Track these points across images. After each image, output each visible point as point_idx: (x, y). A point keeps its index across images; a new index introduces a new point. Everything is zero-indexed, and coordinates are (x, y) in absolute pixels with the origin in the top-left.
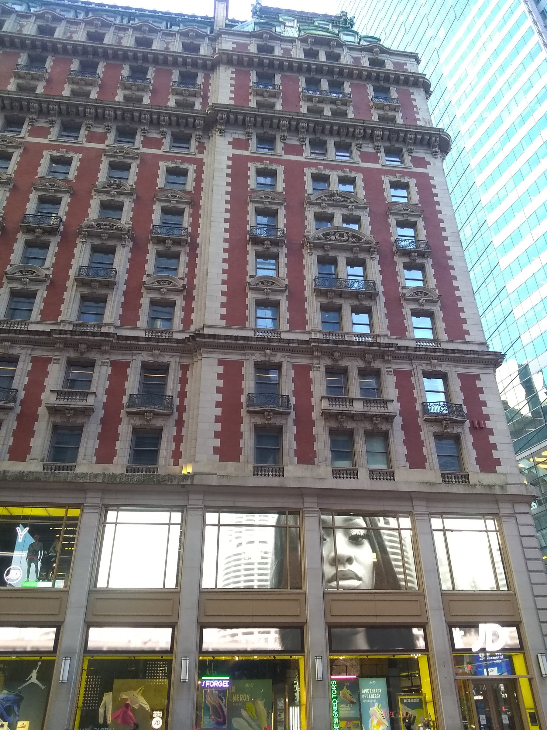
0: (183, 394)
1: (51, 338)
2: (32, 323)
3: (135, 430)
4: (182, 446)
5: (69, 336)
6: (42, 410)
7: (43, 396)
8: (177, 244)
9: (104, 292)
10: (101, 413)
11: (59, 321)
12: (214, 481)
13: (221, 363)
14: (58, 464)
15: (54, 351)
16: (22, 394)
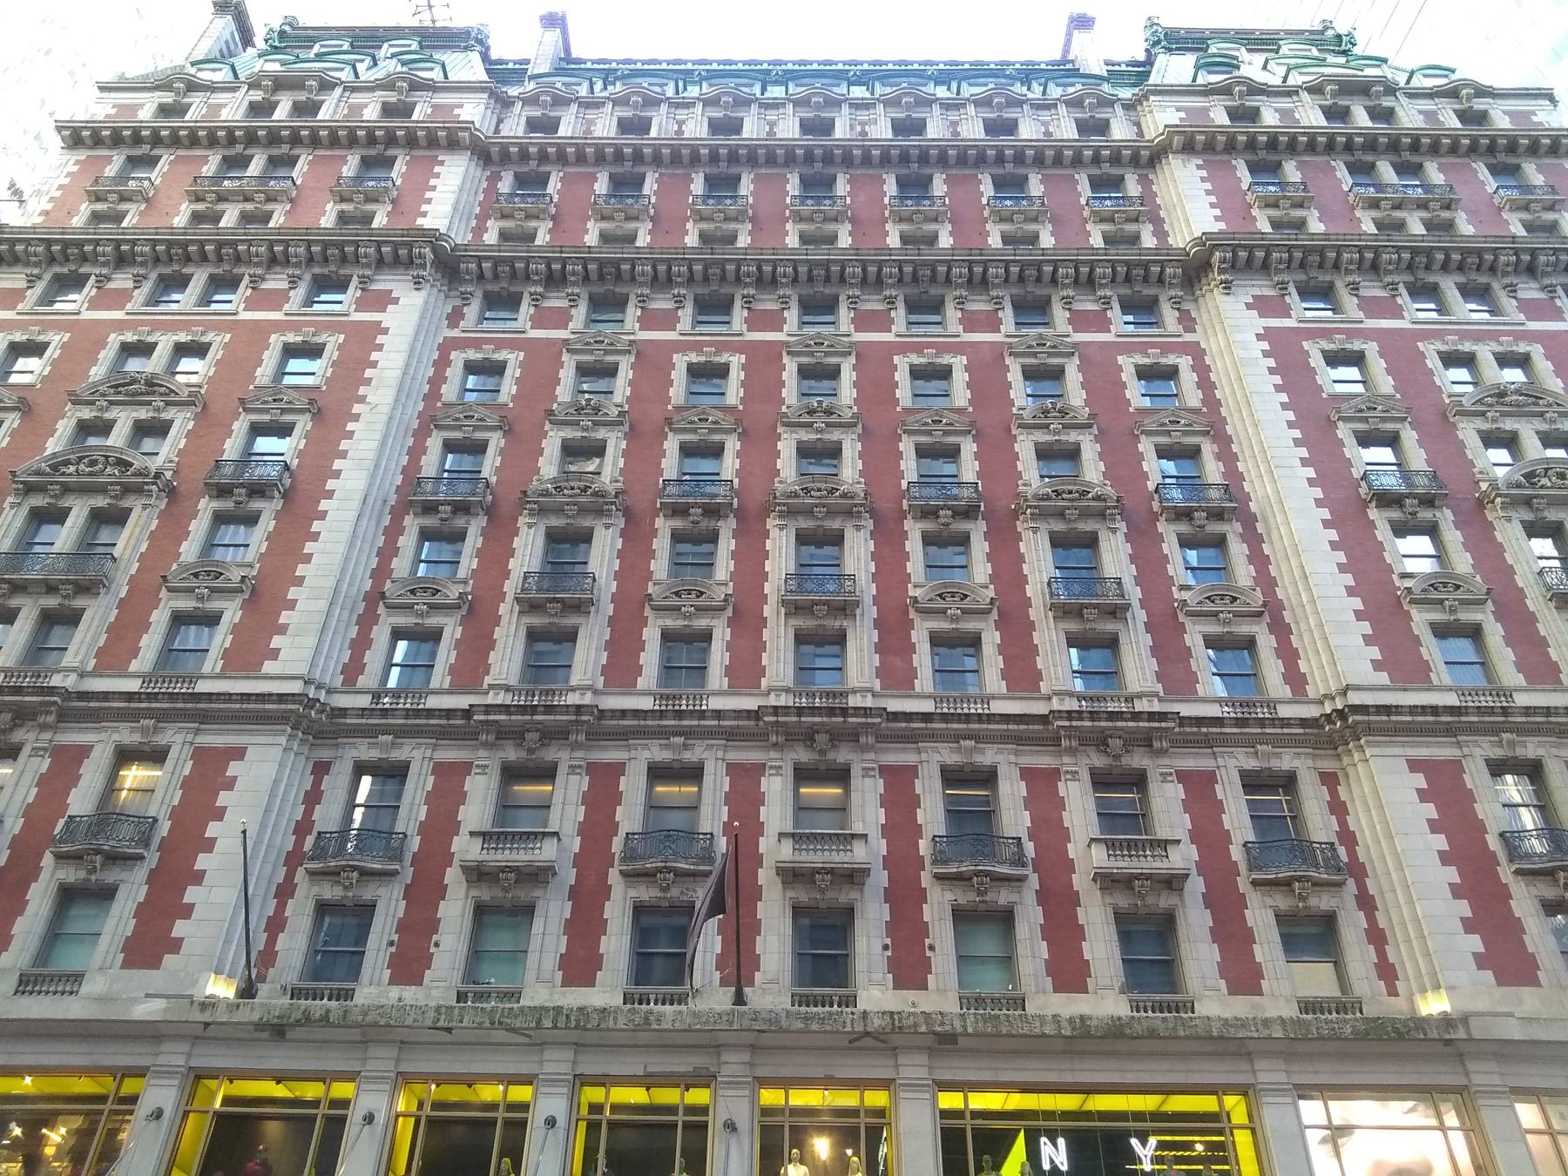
0: (1348, 838)
3: (1281, 918)
5: (1089, 724)
6: (1080, 881)
8: (1215, 519)
9: (1109, 626)
10: (1196, 886)
12: (1514, 1032)
13: (1415, 765)
14: (1158, 997)
15: (1059, 754)
16: (1029, 848)
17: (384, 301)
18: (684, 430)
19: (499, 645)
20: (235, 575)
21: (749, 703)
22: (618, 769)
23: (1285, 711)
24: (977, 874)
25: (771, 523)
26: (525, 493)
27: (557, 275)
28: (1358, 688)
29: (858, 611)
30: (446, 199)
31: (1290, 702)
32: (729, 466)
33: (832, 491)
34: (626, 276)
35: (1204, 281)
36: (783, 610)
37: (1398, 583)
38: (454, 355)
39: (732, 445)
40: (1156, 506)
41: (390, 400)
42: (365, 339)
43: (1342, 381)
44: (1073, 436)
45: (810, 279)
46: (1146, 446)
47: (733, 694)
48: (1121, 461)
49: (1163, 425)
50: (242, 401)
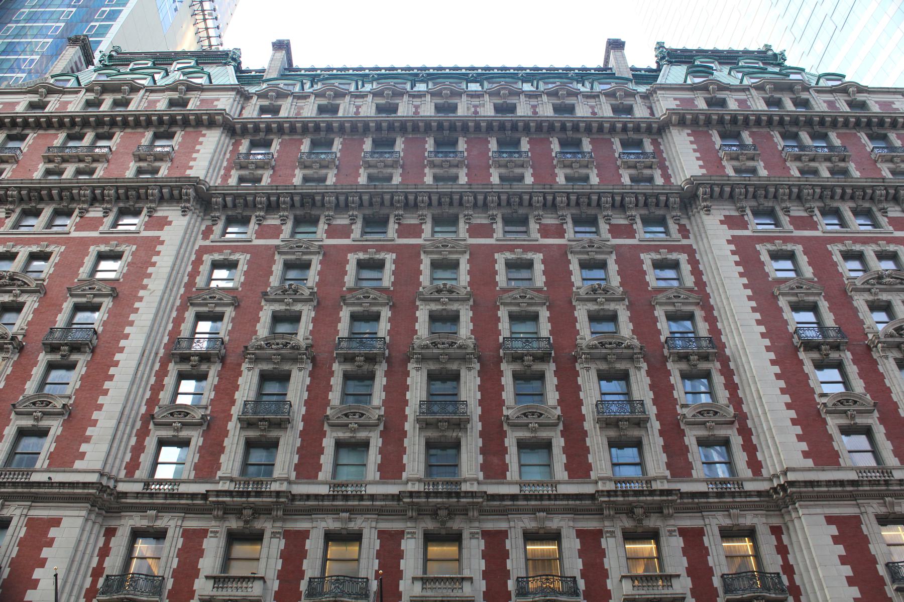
0: (788, 569)
9: (635, 433)
13: (830, 520)
15: (602, 520)
16: (581, 584)
17: (163, 223)
18: (353, 304)
19: (227, 450)
20: (59, 404)
21: (393, 489)
22: (305, 534)
23: (749, 486)
25: (410, 366)
26: (246, 348)
27: (274, 204)
29: (469, 426)
30: (205, 158)
32: (383, 328)
33: (452, 344)
34: (319, 204)
35: (694, 206)
36: (418, 426)
37: (818, 400)
38: (205, 257)
39: (386, 313)
40: (666, 352)
41: (162, 287)
42: (148, 248)
43: (779, 270)
44: (612, 306)
45: (440, 204)
46: (659, 312)
47: (383, 483)
48: (644, 322)
49: (670, 298)
50: (69, 289)
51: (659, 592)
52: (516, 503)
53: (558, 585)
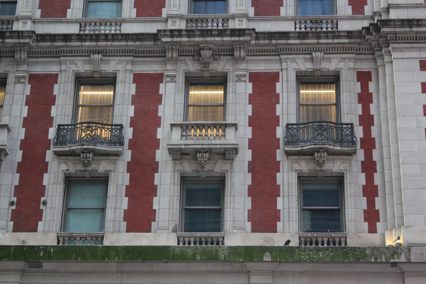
0: (367, 120)
1: (159, 43)
2: (125, 21)
4: (378, 201)
6: (161, 155)
7: (160, 133)
10: (246, 155)
11: (164, 15)
14: (199, 234)
15: (165, 63)
16: (128, 133)
24: (84, 151)
28: (397, 6)
31: (349, 18)
51: (209, 142)
52: (68, 44)
53: (105, 134)
